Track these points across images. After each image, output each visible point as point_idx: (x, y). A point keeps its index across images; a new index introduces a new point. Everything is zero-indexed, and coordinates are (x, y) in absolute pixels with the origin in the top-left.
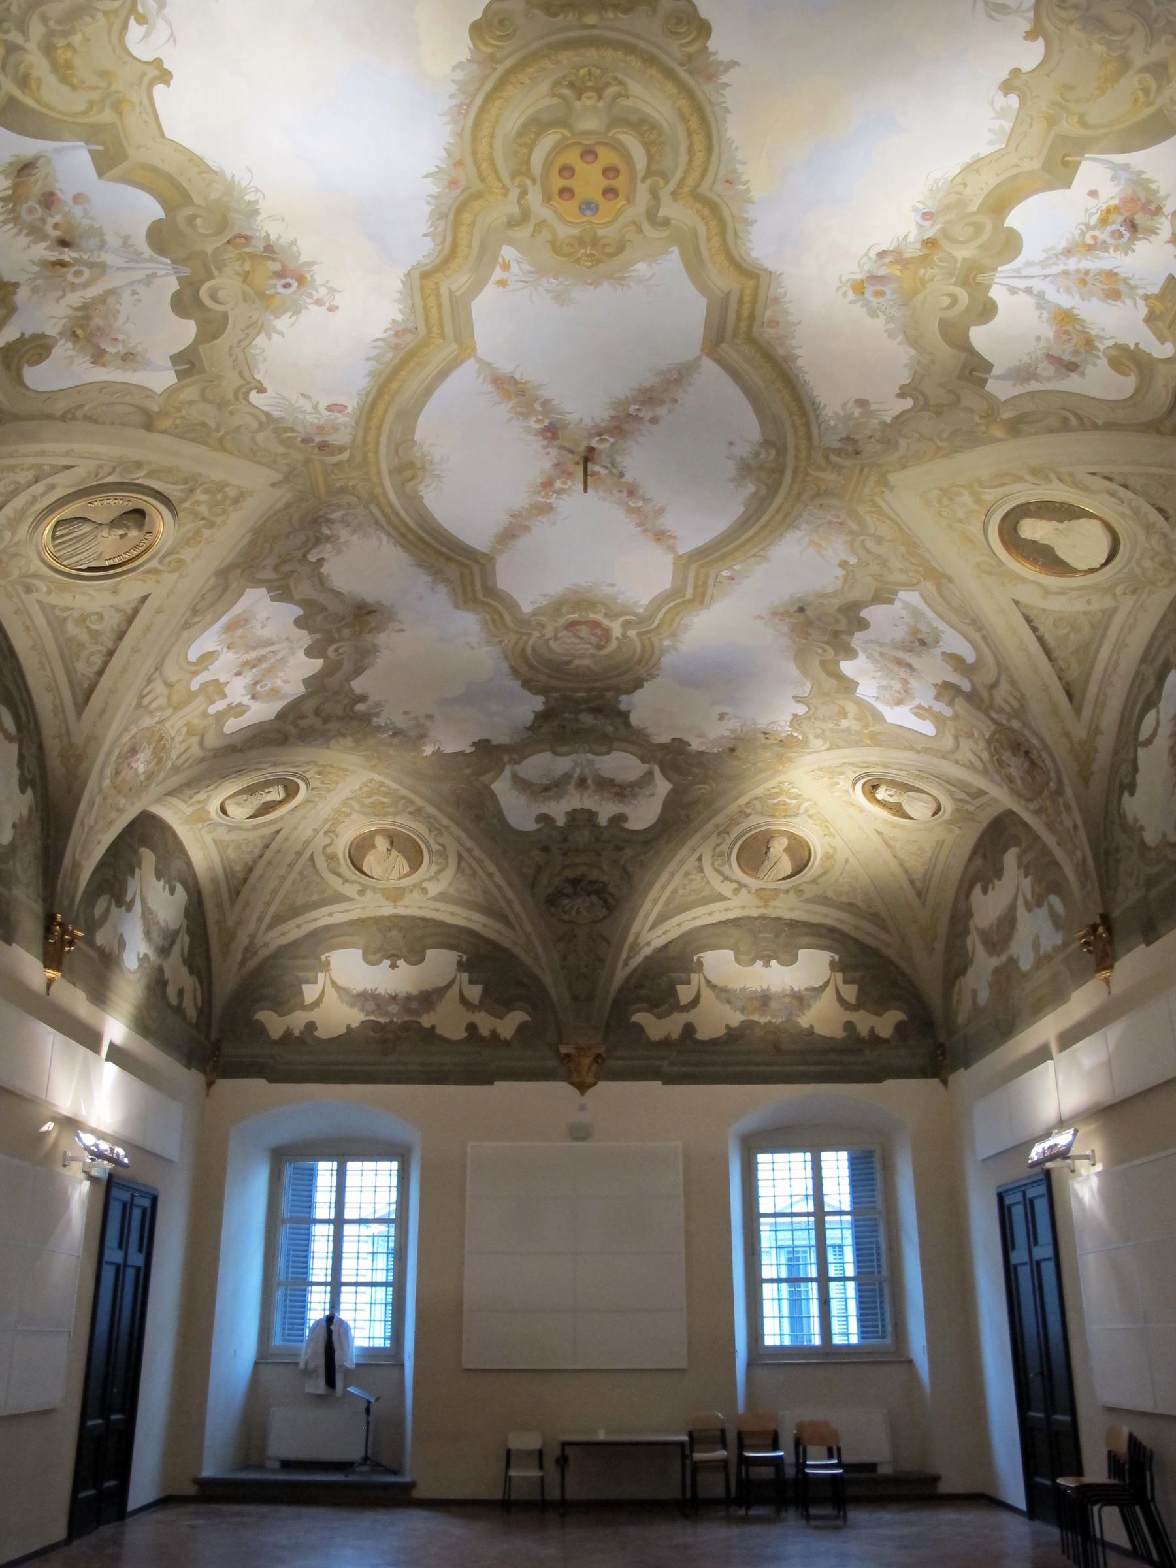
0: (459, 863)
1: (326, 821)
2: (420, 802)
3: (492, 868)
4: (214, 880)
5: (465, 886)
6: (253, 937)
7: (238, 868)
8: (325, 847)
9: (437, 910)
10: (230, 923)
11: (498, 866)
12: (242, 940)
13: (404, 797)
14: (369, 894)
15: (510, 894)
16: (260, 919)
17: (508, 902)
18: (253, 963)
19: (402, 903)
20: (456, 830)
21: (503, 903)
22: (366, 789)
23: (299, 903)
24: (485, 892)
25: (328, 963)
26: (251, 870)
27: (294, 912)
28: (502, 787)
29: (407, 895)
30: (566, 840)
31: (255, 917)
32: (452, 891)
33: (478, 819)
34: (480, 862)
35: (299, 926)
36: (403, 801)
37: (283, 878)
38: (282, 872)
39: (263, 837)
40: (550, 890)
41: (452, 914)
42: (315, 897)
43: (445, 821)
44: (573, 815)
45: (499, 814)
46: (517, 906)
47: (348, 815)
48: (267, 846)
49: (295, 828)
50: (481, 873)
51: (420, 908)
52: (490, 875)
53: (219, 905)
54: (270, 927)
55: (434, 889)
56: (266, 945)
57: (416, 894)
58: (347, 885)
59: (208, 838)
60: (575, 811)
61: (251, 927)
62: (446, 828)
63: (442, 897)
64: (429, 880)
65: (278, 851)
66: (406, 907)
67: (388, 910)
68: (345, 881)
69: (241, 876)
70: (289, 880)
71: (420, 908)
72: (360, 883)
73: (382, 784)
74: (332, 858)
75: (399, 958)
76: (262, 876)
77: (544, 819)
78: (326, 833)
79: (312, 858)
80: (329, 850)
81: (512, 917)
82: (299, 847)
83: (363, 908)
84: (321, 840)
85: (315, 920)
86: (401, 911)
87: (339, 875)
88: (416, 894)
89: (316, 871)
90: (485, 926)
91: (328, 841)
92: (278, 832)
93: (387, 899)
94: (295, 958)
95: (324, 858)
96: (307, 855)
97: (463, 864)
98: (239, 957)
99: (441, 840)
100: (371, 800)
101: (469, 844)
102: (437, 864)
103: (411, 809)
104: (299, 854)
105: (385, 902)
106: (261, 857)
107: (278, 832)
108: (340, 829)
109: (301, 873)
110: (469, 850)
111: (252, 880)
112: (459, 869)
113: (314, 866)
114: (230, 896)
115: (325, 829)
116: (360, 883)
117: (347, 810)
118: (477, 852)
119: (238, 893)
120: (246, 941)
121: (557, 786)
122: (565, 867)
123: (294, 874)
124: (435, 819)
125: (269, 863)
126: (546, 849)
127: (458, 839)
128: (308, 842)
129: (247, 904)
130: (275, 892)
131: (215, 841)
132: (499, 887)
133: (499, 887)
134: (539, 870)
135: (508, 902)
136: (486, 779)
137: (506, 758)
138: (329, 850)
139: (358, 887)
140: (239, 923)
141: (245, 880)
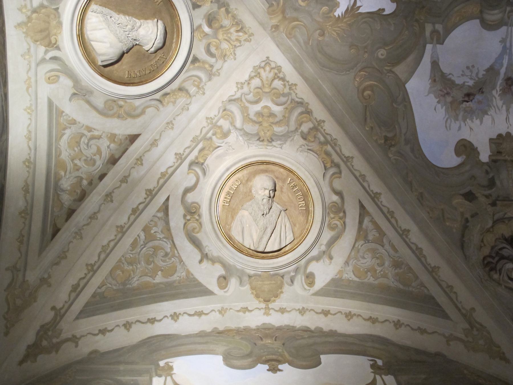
0: (361, 222)
1: (196, 140)
2: (319, 112)
3: (406, 222)
4: (28, 189)
5: (368, 261)
6: (59, 314)
7: (66, 184)
8: (187, 191)
9: (326, 313)
10: (32, 277)
11: (413, 217)
12: (41, 313)
13: (301, 103)
14: (233, 282)
15: (433, 258)
16: (77, 290)
17: (432, 271)
18: (47, 363)
19: (277, 304)
20: (360, 164)
21: (425, 278)
22: (256, 82)
23: (135, 282)
24: (397, 265)
25: (171, 368)
26: (82, 196)
27: (123, 296)
28: (418, 86)
29: (286, 288)
30: (492, 183)
31: (72, 281)
32: (349, 275)
33: (388, 143)
34: (389, 216)
35: (127, 326)
36: (300, 110)
37: (122, 231)
38: (123, 220)
39: (112, 137)
40: (486, 251)
41: (349, 316)
42: (159, 279)
43: (348, 148)
44: (498, 142)
45: (413, 141)
46: (446, 274)
47: (226, 135)
48: (113, 161)
49: (154, 143)
50: (391, 233)
51: (302, 311)
52: (404, 234)
53: (23, 239)
54: (91, 309)
55: (324, 272)
56: (75, 340)
57: (298, 287)
58: (206, 264)
59: (45, 91)
60: (500, 136)
61: (62, 296)
62: (347, 160)
63: (336, 288)
64: (317, 259)
65: (125, 180)
66: (282, 311)
67: (255, 319)
68: (205, 257)
69: (66, 199)
70: (128, 240)
71: (302, 311)
72: (224, 265)
73: (278, 74)
74: (192, 211)
75: (280, 362)
76: (93, 217)
77: (465, 148)
78: (192, 164)
79: (165, 208)
80: (190, 197)
81: (442, 299)
82: (152, 185)
83: (222, 311)
84: (183, 178)
85: (152, 321)
86: (276, 320)
87: (196, 243)
88: (298, 287)
89: (170, 237)
90: (398, 324)
91: (190, 181)
92: (133, 138)
93: (257, 296)
94: (119, 363)
95: (181, 211)
96: (161, 199)
97: (366, 221)
98: (30, 338)
99: (337, 185)
100: (258, 108)
101: (375, 185)
102: (332, 228)
103: (305, 128)
104: (151, 194)
105: (254, 303)
106: (102, 177)
107: (133, 138)
108: (210, 161)
109: (146, 229)
110: (374, 197)
111: (80, 217)
112: (361, 234)
113: (167, 223)
114: (44, 231)
115: (192, 157)
116: (224, 265)
117: (225, 124)
118: (387, 200)
119: (56, 231)
120: (50, 316)
121: (481, 91)
122: (495, 222)
123: (136, 231)
124: (334, 143)
125: (109, 197)
126: (470, 196)
127: (361, 179)
128: (166, 177)
129: (63, 256)
130: (107, 251)
131: (50, 104)
132: (418, 252)
133: (418, 252)
134: (465, 227)
135: (432, 271)
136: (400, 70)
137: (429, 28)
138: (190, 197)
139: (219, 270)
140: (44, 281)
141: (71, 212)
